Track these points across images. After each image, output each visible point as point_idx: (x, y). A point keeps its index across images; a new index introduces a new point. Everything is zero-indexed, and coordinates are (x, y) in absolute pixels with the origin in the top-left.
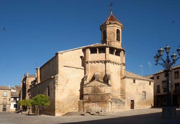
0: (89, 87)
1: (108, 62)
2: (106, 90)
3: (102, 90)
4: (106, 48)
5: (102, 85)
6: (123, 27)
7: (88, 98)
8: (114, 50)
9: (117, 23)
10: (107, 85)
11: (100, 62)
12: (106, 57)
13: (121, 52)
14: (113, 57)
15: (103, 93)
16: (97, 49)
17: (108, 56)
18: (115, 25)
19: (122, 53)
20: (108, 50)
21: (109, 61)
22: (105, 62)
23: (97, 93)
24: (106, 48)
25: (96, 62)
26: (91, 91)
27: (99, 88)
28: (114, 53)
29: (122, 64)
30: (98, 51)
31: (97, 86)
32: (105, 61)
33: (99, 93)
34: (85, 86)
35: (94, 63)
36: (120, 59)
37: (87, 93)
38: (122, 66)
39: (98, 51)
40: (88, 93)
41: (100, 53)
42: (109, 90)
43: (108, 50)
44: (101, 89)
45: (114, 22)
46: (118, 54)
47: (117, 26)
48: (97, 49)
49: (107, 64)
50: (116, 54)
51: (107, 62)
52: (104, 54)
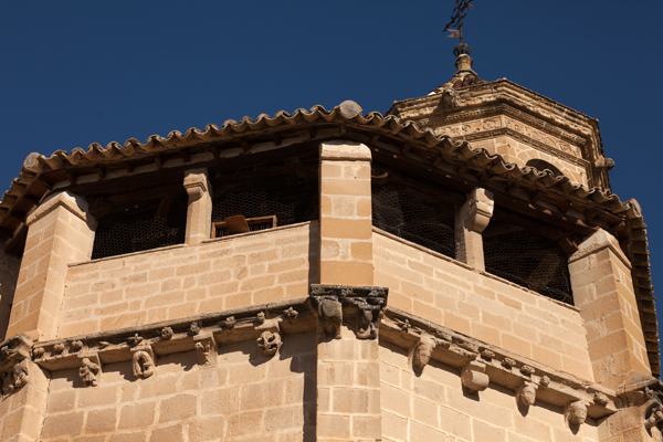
1: (357, 322)
4: (327, 149)
6: (600, 161)
8: (466, 194)
9: (525, 100)
11: (223, 347)
12: (326, 255)
13: (584, 246)
14: (451, 289)
16: (196, 180)
17: (366, 250)
18: (503, 121)
19: (599, 264)
20: (346, 176)
21: (364, 310)
22: (304, 328)
24: (327, 149)
25: (160, 359)
28: (474, 242)
29: (622, 400)
30: (201, 212)
32: (307, 308)
35: (126, 366)
36: (581, 344)
38: (628, 431)
39: (201, 212)
41: (222, 231)
43: (346, 176)
45: (488, 97)
46: (533, 244)
47: (526, 130)
48: (196, 180)
49: (344, 354)
50: (497, 265)
51: (332, 334)
52: (302, 231)
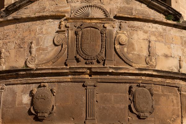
0: (37, 26)
2: (160, 49)
3: (131, 45)
5: (135, 14)
7: (26, 99)
10: (161, 17)
15: (143, 65)
23: (95, 66)
26: (52, 51)
27: (113, 27)
31: (99, 14)
33: (110, 67)
34: (10, 17)
37: (20, 64)
40: (31, 66)
42: (177, 51)
44: (123, 38)
